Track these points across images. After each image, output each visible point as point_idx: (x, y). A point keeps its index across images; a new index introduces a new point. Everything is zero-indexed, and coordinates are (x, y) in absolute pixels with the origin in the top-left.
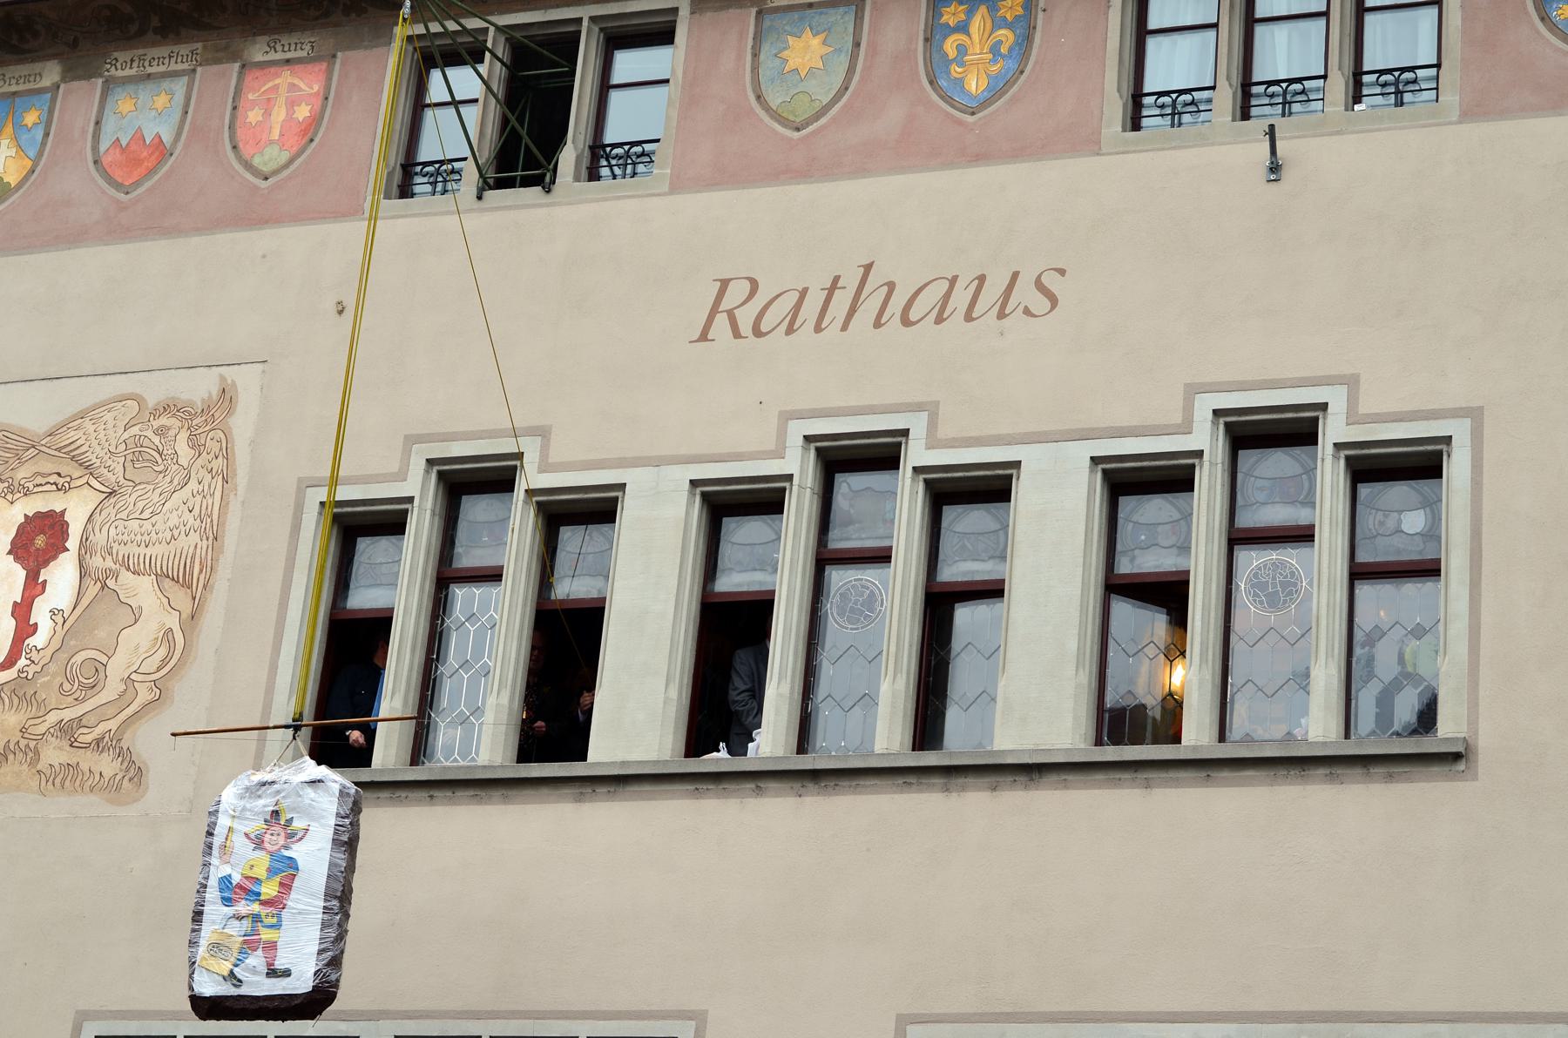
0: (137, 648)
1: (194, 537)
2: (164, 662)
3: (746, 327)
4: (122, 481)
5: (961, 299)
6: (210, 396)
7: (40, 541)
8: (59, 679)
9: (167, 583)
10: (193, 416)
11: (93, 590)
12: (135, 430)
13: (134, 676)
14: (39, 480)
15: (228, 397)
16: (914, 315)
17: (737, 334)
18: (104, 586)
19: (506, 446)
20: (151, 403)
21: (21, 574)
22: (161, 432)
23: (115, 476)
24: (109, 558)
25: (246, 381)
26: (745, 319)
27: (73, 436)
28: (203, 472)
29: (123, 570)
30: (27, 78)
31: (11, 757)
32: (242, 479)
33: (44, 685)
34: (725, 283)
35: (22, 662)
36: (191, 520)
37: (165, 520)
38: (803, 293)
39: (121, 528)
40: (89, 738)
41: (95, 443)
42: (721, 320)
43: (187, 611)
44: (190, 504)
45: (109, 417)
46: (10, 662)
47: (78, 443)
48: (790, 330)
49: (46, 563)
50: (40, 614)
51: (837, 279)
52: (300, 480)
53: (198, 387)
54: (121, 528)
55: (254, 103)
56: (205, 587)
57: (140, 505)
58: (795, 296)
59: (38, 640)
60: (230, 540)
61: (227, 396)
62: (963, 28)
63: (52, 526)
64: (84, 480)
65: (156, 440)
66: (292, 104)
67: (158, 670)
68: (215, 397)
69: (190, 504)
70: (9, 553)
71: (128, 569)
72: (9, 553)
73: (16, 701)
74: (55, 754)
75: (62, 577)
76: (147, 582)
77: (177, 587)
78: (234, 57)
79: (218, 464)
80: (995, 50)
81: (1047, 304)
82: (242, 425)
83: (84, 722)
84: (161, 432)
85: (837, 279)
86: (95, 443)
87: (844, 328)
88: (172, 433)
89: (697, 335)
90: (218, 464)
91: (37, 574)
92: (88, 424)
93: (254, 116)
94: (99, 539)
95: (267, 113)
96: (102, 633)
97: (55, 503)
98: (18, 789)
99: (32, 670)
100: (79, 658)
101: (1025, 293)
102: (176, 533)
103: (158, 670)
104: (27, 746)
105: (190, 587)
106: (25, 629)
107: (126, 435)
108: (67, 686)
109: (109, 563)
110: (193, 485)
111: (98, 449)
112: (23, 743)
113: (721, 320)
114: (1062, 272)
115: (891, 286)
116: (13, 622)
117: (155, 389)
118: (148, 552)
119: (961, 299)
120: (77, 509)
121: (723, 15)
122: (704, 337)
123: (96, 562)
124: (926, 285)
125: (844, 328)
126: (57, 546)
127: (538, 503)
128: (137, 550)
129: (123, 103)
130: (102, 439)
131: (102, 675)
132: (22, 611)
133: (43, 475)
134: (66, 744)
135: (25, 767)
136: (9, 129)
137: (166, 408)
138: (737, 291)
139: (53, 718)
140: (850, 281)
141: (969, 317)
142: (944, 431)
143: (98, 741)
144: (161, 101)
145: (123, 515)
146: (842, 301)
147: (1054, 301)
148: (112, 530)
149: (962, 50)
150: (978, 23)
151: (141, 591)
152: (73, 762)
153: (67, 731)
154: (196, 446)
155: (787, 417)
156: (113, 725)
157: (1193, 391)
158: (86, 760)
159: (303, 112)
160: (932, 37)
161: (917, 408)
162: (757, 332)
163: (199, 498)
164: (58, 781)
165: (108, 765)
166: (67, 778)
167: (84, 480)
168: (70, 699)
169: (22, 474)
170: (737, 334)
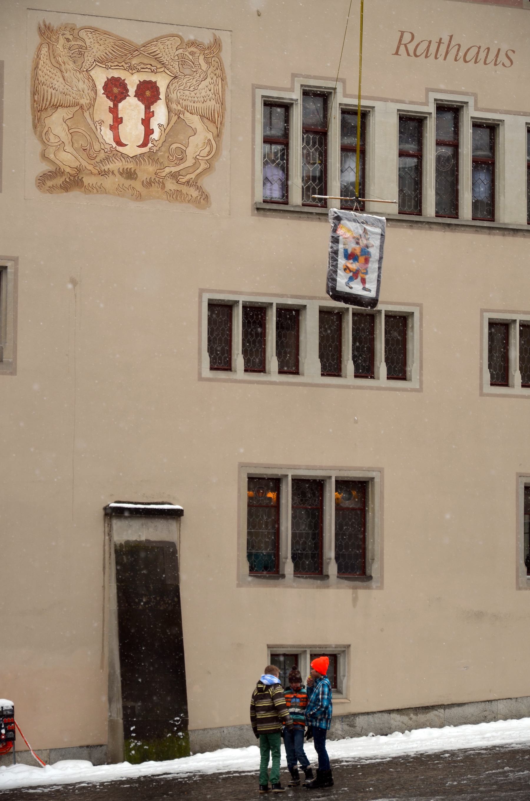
0: (197, 145)
1: (213, 102)
2: (209, 153)
3: (411, 52)
4: (179, 73)
5: (482, 55)
6: (210, 42)
7: (148, 93)
8: (167, 155)
9: (206, 120)
10: (204, 49)
11: (174, 119)
12: (180, 51)
13: (198, 157)
14: (142, 66)
15: (218, 43)
16: (468, 59)
17: (408, 55)
18: (179, 117)
19: (330, 84)
20: (186, 40)
21: (143, 107)
22: (192, 53)
24: (179, 105)
25: (225, 38)
26: (411, 47)
27: (154, 49)
28: (212, 75)
29: (186, 111)
31: (153, 184)
32: (229, 80)
33: (161, 155)
34: (402, 33)
35: (150, 145)
36: (211, 95)
37: (201, 92)
38: (430, 42)
39: (182, 93)
40: (184, 180)
41: (164, 54)
42: (402, 48)
43: (215, 134)
44: (209, 87)
45: (168, 43)
47: (158, 52)
48: (426, 57)
49: (152, 103)
50: (154, 125)
51: (441, 39)
52: (253, 85)
54: (182, 93)
56: (221, 123)
57: (189, 84)
58: (427, 43)
59: (155, 136)
60: (228, 105)
61: (217, 44)
63: (152, 88)
64: (162, 70)
65: (191, 57)
67: (208, 155)
68: (212, 42)
69: (209, 87)
70: (135, 96)
71: (188, 111)
72: (135, 96)
73: (151, 161)
74: (171, 185)
75: (160, 111)
77: (209, 122)
79: (218, 72)
81: (509, 63)
83: (181, 173)
84: (192, 53)
85: (441, 39)
86: (164, 54)
87: (445, 59)
88: (197, 55)
89: (394, 53)
90: (218, 72)
91: (149, 108)
92: (159, 44)
94: (173, 96)
97: (152, 78)
98: (158, 198)
99: (155, 149)
100: (174, 146)
102: (205, 99)
103: (208, 155)
104: (159, 180)
105: (215, 123)
106: (149, 132)
107: (177, 53)
108: (171, 158)
109: (179, 108)
110: (209, 79)
111: (166, 57)
112: (157, 179)
113: (402, 48)
114: (514, 52)
115: (459, 46)
116: (142, 128)
118: (195, 105)
119: (482, 55)
120: (162, 82)
122: (397, 53)
123: (174, 106)
124: (471, 47)
125: (445, 59)
126: (155, 97)
127: (341, 108)
128: (191, 104)
130: (168, 51)
131: (184, 155)
132: (146, 122)
133: (144, 64)
134: (175, 182)
135: (160, 189)
137: (193, 44)
138: (407, 37)
139: (167, 170)
140: (446, 40)
141: (485, 63)
142: (480, 105)
143: (188, 182)
145: (182, 88)
146: (443, 49)
147: (512, 63)
148: (178, 93)
151: (195, 121)
152: (179, 189)
153: (175, 176)
154: (208, 63)
155: (428, 90)
156: (193, 176)
158: (185, 189)
162: (416, 56)
163: (212, 86)
164: (174, 196)
165: (194, 193)
166: (176, 196)
167: (162, 70)
168: (173, 163)
169: (134, 62)
170: (408, 55)
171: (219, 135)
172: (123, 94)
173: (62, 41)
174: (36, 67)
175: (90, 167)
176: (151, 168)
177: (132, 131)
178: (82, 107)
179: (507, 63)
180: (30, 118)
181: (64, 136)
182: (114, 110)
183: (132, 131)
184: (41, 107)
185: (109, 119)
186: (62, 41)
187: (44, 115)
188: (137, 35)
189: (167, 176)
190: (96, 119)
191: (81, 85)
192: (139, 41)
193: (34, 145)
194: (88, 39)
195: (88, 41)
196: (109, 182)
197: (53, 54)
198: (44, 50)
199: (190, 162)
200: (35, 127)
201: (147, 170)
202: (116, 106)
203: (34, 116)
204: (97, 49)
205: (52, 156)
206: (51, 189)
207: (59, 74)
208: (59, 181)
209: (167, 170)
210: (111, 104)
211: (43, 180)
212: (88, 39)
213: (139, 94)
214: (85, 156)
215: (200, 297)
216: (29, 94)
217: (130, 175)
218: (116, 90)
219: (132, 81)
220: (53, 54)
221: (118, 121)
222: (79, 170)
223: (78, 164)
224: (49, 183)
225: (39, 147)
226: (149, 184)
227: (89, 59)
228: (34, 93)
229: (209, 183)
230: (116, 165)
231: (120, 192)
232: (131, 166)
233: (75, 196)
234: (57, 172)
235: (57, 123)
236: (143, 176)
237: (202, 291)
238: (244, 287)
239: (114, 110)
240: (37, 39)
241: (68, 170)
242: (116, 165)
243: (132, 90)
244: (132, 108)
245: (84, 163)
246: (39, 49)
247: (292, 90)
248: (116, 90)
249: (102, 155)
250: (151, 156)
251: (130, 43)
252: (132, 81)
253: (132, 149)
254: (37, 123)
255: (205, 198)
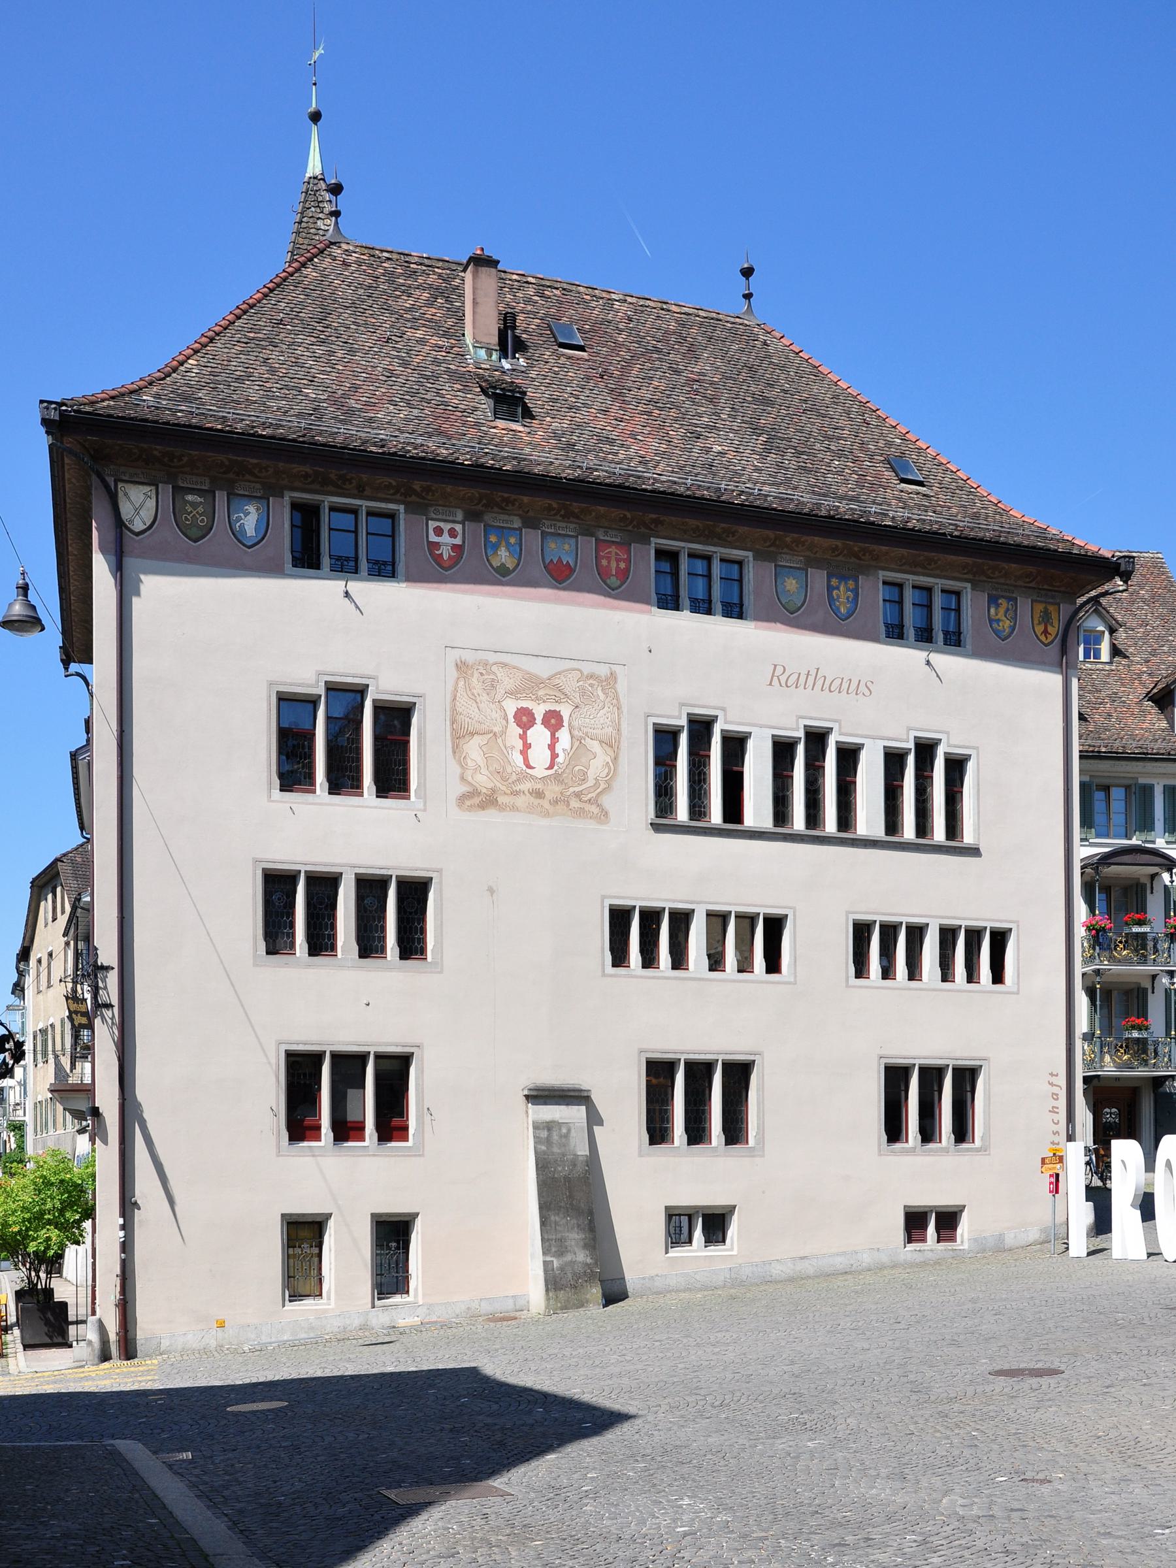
1: (611, 729)
3: (783, 683)
5: (845, 686)
7: (553, 721)
22: (591, 685)
23: (577, 700)
26: (783, 679)
30: (507, 522)
32: (625, 710)
37: (598, 719)
46: (551, 767)
50: (559, 749)
53: (603, 671)
55: (603, 557)
59: (560, 759)
61: (613, 676)
62: (838, 588)
66: (618, 561)
74: (575, 804)
75: (564, 735)
76: (596, 743)
78: (592, 535)
80: (848, 598)
82: (622, 686)
84: (591, 685)
93: (604, 562)
94: (575, 724)
95: (609, 562)
96: (583, 760)
99: (560, 771)
101: (862, 688)
106: (554, 756)
113: (775, 679)
116: (549, 753)
117: (587, 668)
119: (845, 686)
120: (565, 711)
121: (766, 563)
123: (576, 733)
126: (559, 724)
129: (552, 545)
130: (570, 684)
132: (552, 747)
136: (503, 543)
137: (591, 676)
138: (779, 670)
139: (571, 790)
140: (813, 673)
142: (843, 730)
144: (566, 547)
146: (811, 679)
149: (839, 597)
150: (842, 588)
151: (595, 746)
153: (578, 795)
156: (594, 795)
157: (909, 729)
158: (587, 807)
159: (622, 565)
160: (830, 589)
161: (835, 721)
165: (594, 809)
166: (580, 813)
169: (541, 693)
171: (615, 759)
172: (532, 722)
173: (476, 674)
174: (455, 699)
175: (504, 788)
176: (558, 788)
177: (540, 755)
178: (495, 734)
179: (867, 692)
180: (449, 744)
181: (481, 761)
182: (523, 737)
183: (540, 755)
184: (459, 735)
185: (519, 744)
186: (476, 674)
187: (462, 741)
188: (542, 669)
189: (572, 796)
190: (508, 745)
191: (494, 715)
192: (545, 675)
193: (454, 769)
194: (500, 673)
195: (499, 675)
196: (521, 801)
197: (469, 687)
198: (461, 683)
199: (591, 782)
200: (454, 752)
201: (553, 790)
202: (525, 733)
203: (453, 743)
204: (507, 682)
205: (470, 779)
206: (471, 808)
207: (474, 705)
208: (476, 800)
209: (571, 790)
210: (521, 731)
211: (462, 799)
212: (500, 673)
213: (546, 722)
214: (499, 778)
215: (602, 902)
216: (448, 723)
217: (539, 794)
218: (525, 719)
219: (539, 711)
220: (469, 687)
221: (527, 746)
222: (493, 790)
223: (492, 785)
224: (468, 803)
225: (459, 770)
226: (556, 802)
227: (501, 691)
228: (453, 722)
229: (606, 801)
230: (526, 786)
231: (530, 810)
232: (539, 786)
233: (491, 816)
234: (474, 793)
235: (474, 749)
236: (549, 795)
237: (603, 897)
238: (639, 894)
239: (523, 737)
240: (455, 674)
241: (484, 790)
242: (526, 786)
243: (539, 718)
244: (539, 735)
245: (498, 785)
246: (457, 683)
247: (680, 718)
248: (525, 719)
249: (514, 777)
250: (557, 778)
251: (537, 676)
252: (539, 711)
253: (540, 771)
254: (456, 749)
255: (605, 813)
